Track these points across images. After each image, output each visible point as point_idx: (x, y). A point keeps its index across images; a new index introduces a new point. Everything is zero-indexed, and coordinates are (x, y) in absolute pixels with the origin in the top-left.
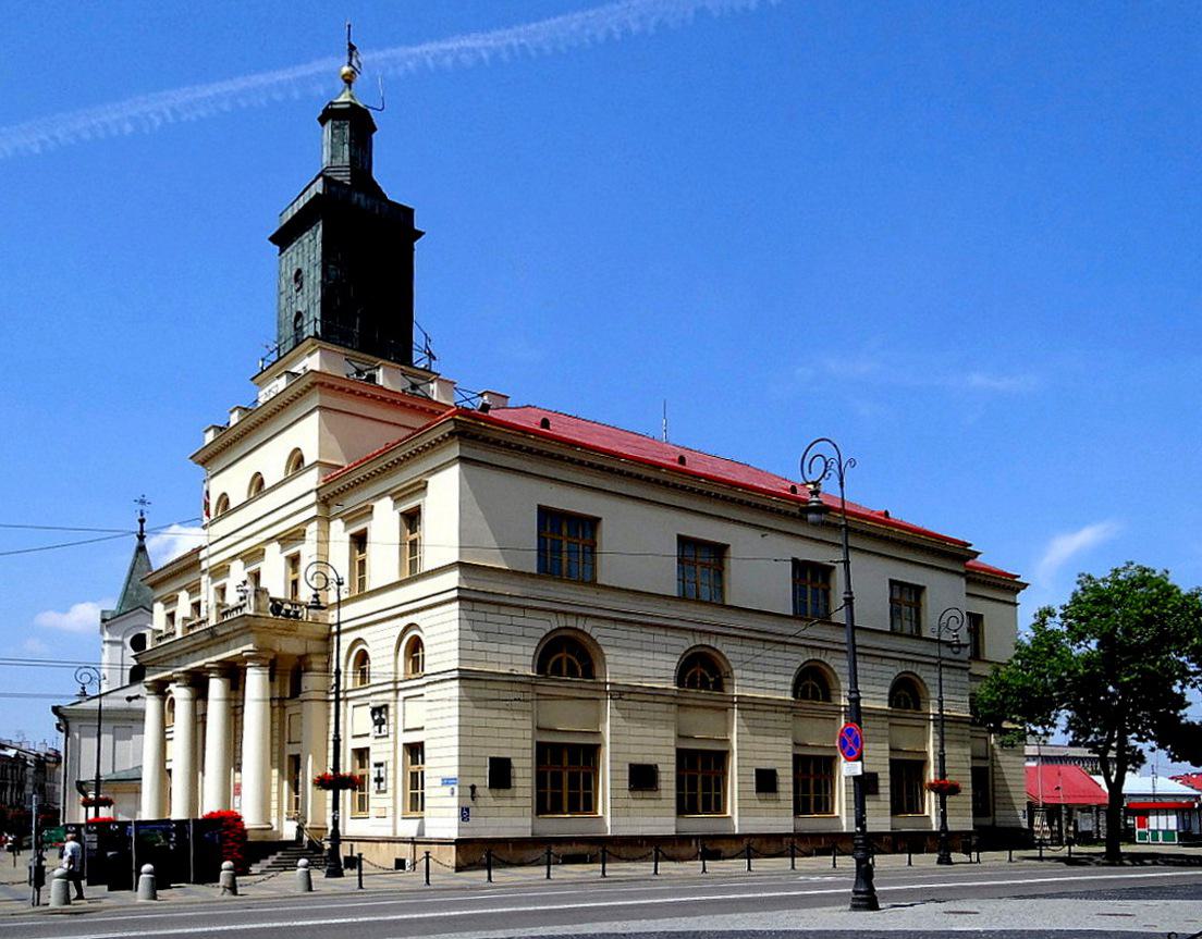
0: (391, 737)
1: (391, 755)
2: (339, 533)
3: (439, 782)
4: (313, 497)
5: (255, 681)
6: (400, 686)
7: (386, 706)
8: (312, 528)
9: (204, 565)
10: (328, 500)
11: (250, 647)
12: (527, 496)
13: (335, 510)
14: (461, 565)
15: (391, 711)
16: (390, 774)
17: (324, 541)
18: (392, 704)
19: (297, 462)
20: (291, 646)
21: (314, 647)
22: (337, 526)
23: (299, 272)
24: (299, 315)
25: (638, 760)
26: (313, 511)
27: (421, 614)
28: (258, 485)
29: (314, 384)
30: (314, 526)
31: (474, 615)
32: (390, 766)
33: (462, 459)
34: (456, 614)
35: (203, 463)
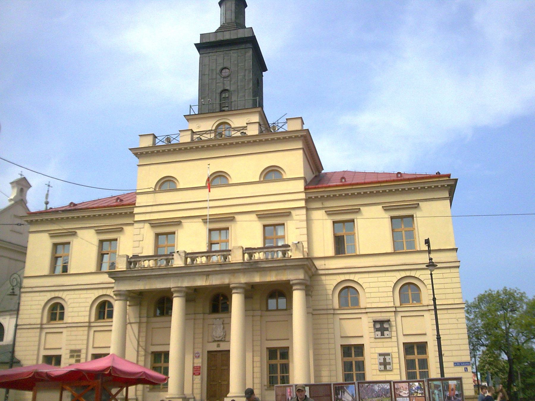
0: (394, 339)
1: (396, 349)
3: (453, 363)
6: (398, 309)
7: (388, 321)
9: (137, 218)
11: (302, 276)
15: (393, 323)
16: (396, 360)
18: (392, 319)
19: (272, 174)
22: (319, 215)
24: (225, 91)
28: (218, 179)
29: (302, 136)
32: (395, 355)
35: (136, 154)
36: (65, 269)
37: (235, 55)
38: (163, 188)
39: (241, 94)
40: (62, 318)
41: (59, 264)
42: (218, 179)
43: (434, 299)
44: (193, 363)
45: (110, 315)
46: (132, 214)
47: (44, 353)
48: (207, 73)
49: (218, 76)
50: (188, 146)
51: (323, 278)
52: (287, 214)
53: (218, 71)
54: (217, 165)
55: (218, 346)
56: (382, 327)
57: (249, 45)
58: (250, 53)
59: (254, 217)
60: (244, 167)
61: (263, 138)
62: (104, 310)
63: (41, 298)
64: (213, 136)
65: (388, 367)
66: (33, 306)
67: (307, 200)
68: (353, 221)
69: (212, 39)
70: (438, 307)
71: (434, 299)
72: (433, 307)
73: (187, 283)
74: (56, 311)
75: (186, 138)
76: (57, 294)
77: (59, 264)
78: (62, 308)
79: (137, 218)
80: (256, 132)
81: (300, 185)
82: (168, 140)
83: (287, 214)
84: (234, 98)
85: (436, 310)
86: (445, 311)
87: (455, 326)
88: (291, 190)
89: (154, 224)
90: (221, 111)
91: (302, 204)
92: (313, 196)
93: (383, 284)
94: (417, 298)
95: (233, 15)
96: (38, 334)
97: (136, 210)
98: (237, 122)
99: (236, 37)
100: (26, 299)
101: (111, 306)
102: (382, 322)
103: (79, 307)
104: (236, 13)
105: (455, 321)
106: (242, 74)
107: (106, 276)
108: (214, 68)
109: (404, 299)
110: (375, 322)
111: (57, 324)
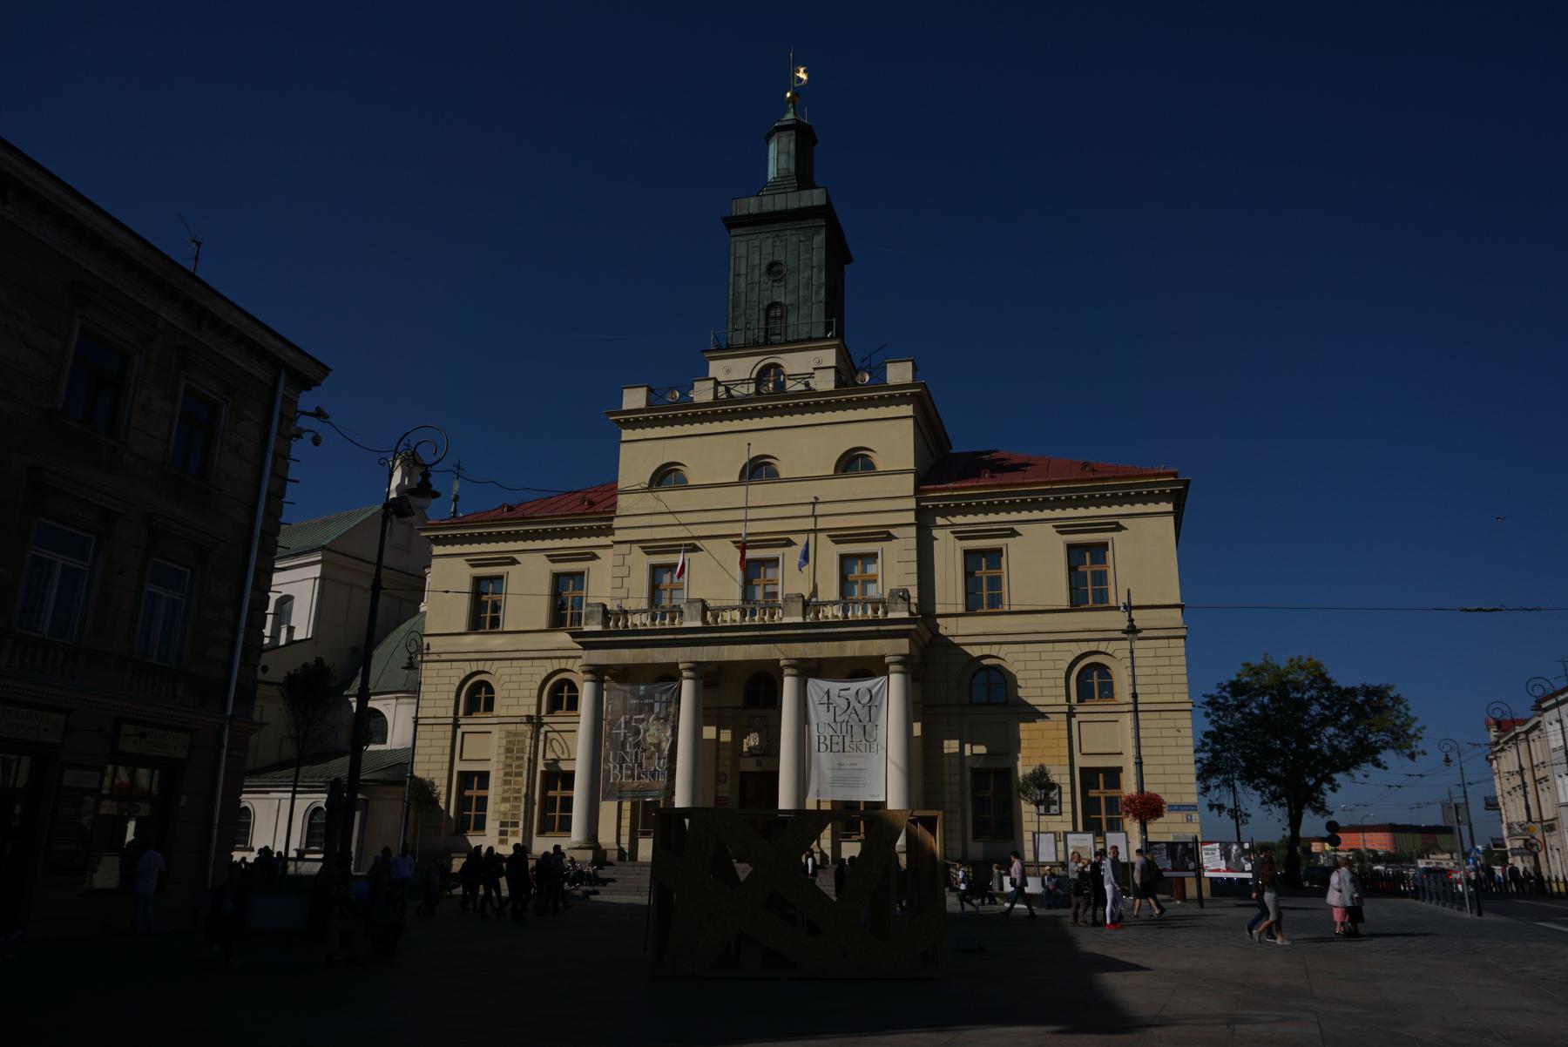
1: (1067, 779)
8: (913, 531)
9: (619, 535)
16: (1066, 798)
24: (774, 305)
28: (758, 470)
36: (495, 622)
37: (794, 239)
39: (804, 311)
40: (489, 706)
41: (484, 612)
42: (758, 470)
43: (1135, 695)
44: (717, 791)
45: (573, 704)
47: (459, 766)
48: (743, 271)
49: (764, 278)
50: (709, 410)
53: (763, 269)
54: (761, 445)
55: (759, 764)
57: (820, 222)
58: (820, 239)
61: (843, 398)
62: (560, 695)
63: (452, 673)
64: (752, 388)
65: (1054, 809)
66: (440, 685)
67: (919, 511)
68: (999, 551)
70: (1140, 707)
71: (1135, 695)
72: (1131, 708)
74: (477, 696)
76: (481, 666)
77: (484, 612)
78: (490, 690)
79: (619, 535)
80: (831, 386)
84: (792, 319)
85: (1136, 711)
86: (1156, 715)
87: (1172, 742)
88: (891, 491)
89: (650, 548)
90: (768, 343)
91: (910, 517)
93: (1051, 665)
94: (1108, 690)
95: (792, 161)
96: (449, 735)
97: (616, 523)
98: (795, 363)
99: (796, 206)
100: (429, 672)
101: (573, 688)
103: (517, 692)
104: (797, 157)
105: (1173, 732)
106: (807, 274)
107: (568, 637)
108: (757, 261)
109: (1085, 693)
111: (480, 718)
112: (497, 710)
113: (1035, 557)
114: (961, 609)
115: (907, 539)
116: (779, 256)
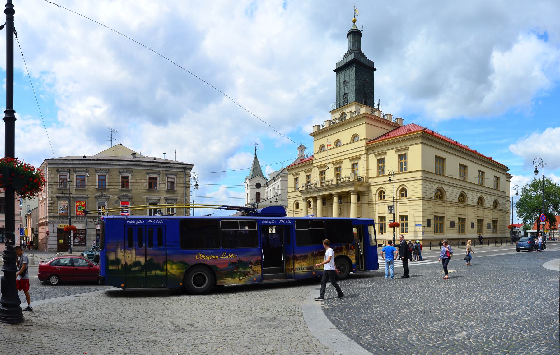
2: (373, 159)
4: (364, 148)
5: (353, 198)
8: (365, 156)
9: (314, 165)
10: (368, 150)
11: (353, 189)
12: (434, 152)
13: (370, 152)
14: (422, 170)
17: (367, 160)
19: (355, 137)
20: (361, 189)
21: (365, 189)
23: (345, 81)
24: (345, 94)
25: (451, 220)
26: (364, 152)
27: (406, 183)
28: (338, 143)
30: (365, 156)
31: (425, 184)
33: (422, 143)
34: (421, 183)
38: (323, 150)
46: (312, 164)
51: (372, 187)
52: (358, 158)
56: (391, 208)
59: (348, 160)
60: (345, 135)
67: (367, 150)
68: (384, 158)
69: (341, 65)
73: (321, 194)
75: (326, 125)
79: (314, 165)
81: (363, 143)
82: (323, 126)
83: (358, 158)
89: (319, 167)
91: (364, 152)
92: (369, 147)
97: (314, 162)
102: (391, 207)
110: (389, 207)
111: (298, 210)
112: (386, 199)
113: (391, 160)
114: (375, 175)
115: (363, 158)
116: (346, 79)
